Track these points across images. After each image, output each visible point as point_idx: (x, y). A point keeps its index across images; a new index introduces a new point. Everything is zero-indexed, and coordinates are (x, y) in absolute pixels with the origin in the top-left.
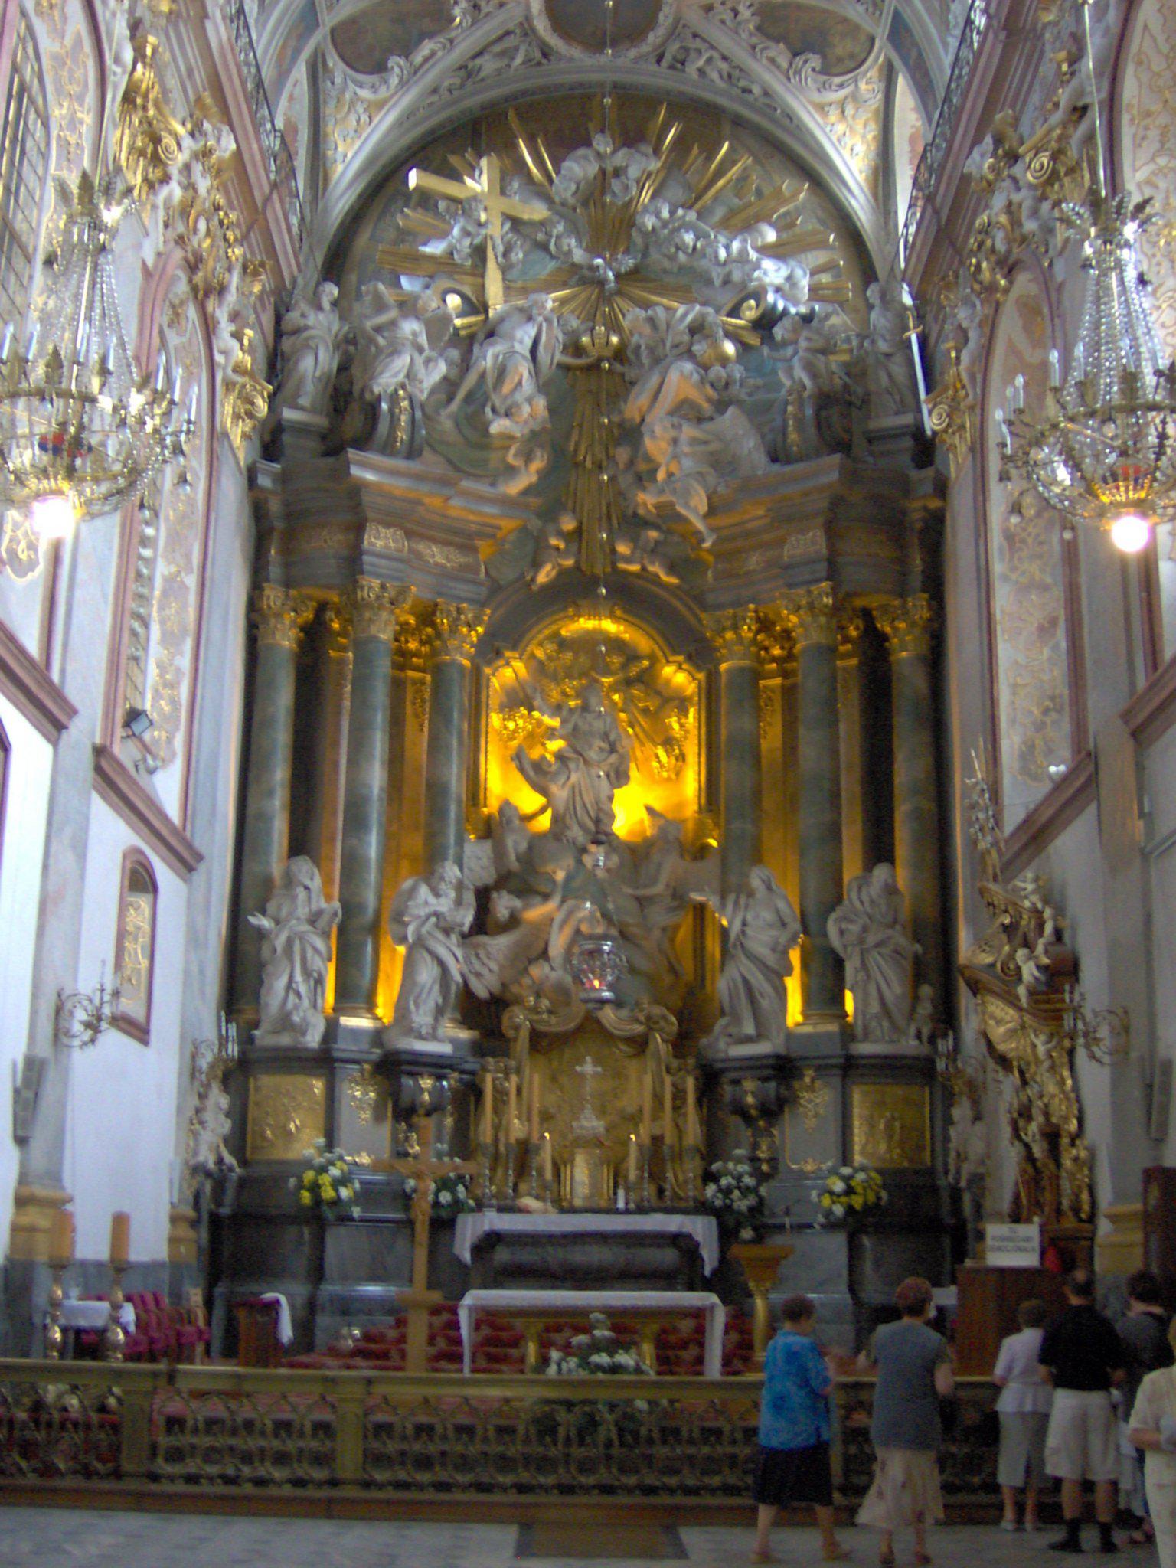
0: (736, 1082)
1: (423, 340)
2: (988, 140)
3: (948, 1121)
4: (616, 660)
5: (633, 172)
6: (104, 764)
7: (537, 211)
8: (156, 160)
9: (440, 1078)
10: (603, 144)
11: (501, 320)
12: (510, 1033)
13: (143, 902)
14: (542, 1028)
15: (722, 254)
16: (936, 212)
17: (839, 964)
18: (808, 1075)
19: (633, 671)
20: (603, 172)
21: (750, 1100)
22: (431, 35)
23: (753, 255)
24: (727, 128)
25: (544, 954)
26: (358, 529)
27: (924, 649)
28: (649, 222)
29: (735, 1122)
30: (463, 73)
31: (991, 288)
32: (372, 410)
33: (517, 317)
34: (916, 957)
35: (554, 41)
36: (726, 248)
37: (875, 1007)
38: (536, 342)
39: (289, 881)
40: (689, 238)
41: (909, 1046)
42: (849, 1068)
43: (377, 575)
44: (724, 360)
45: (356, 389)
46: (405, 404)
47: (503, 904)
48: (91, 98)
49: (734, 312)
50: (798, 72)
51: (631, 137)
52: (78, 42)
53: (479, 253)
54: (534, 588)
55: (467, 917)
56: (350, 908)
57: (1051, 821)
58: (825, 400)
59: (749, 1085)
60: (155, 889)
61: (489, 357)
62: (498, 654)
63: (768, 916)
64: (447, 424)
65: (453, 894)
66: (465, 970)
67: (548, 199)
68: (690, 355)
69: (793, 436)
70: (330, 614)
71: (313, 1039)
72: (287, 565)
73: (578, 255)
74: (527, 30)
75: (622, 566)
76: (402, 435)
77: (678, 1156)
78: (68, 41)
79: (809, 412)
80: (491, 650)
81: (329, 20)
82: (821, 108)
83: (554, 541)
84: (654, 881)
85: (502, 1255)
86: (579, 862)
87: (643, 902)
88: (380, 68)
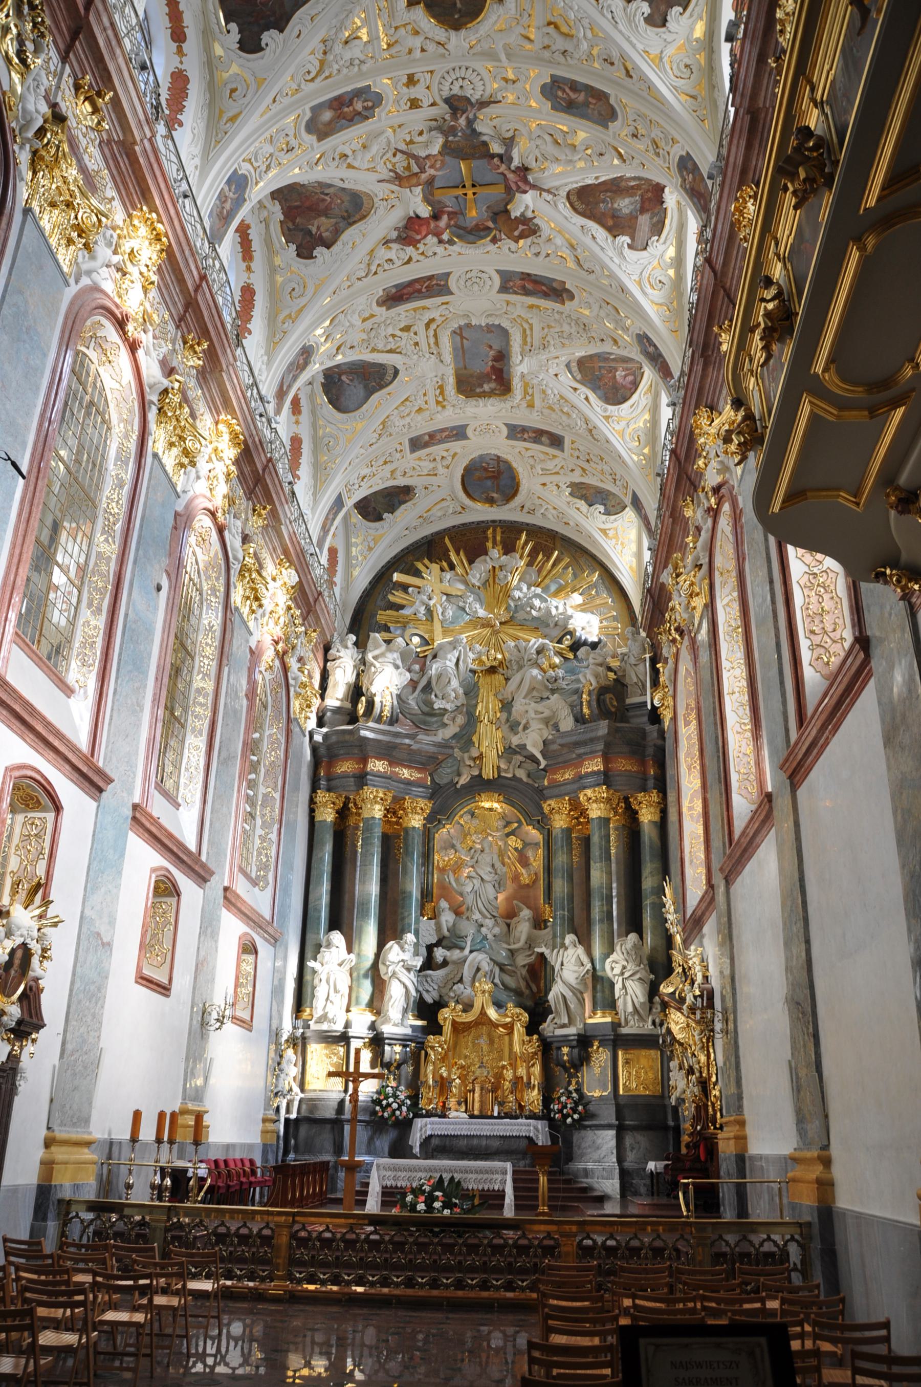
0: (559, 1048)
1: (399, 662)
2: (670, 566)
3: (669, 1070)
4: (501, 823)
5: (508, 568)
6: (228, 894)
8: (257, 599)
9: (405, 1046)
10: (495, 553)
11: (441, 646)
12: (442, 1023)
13: (251, 958)
14: (458, 1020)
16: (652, 597)
17: (612, 985)
18: (596, 1043)
19: (508, 830)
20: (494, 568)
21: (565, 1058)
22: (405, 502)
24: (558, 544)
25: (461, 981)
26: (364, 761)
27: (657, 818)
28: (517, 594)
29: (558, 1070)
30: (421, 520)
31: (674, 641)
33: (449, 647)
34: (652, 981)
35: (467, 501)
36: (557, 606)
37: (630, 1009)
38: (458, 660)
39: (329, 945)
40: (537, 603)
41: (648, 1027)
43: (374, 786)
44: (553, 667)
45: (364, 690)
47: (440, 954)
48: (222, 580)
49: (560, 641)
50: (592, 514)
51: (509, 548)
52: (216, 554)
54: (458, 786)
55: (418, 962)
57: (703, 914)
58: (602, 691)
59: (565, 1050)
60: (256, 953)
61: (434, 668)
62: (440, 821)
64: (413, 703)
65: (412, 950)
66: (420, 989)
67: (466, 583)
69: (586, 710)
70: (351, 805)
72: (329, 780)
73: (481, 613)
75: (503, 774)
77: (529, 1086)
78: (212, 555)
79: (594, 697)
81: (349, 503)
82: (604, 531)
83: (468, 763)
84: (519, 940)
85: (435, 1142)
86: (479, 931)
87: (512, 952)
88: (379, 518)
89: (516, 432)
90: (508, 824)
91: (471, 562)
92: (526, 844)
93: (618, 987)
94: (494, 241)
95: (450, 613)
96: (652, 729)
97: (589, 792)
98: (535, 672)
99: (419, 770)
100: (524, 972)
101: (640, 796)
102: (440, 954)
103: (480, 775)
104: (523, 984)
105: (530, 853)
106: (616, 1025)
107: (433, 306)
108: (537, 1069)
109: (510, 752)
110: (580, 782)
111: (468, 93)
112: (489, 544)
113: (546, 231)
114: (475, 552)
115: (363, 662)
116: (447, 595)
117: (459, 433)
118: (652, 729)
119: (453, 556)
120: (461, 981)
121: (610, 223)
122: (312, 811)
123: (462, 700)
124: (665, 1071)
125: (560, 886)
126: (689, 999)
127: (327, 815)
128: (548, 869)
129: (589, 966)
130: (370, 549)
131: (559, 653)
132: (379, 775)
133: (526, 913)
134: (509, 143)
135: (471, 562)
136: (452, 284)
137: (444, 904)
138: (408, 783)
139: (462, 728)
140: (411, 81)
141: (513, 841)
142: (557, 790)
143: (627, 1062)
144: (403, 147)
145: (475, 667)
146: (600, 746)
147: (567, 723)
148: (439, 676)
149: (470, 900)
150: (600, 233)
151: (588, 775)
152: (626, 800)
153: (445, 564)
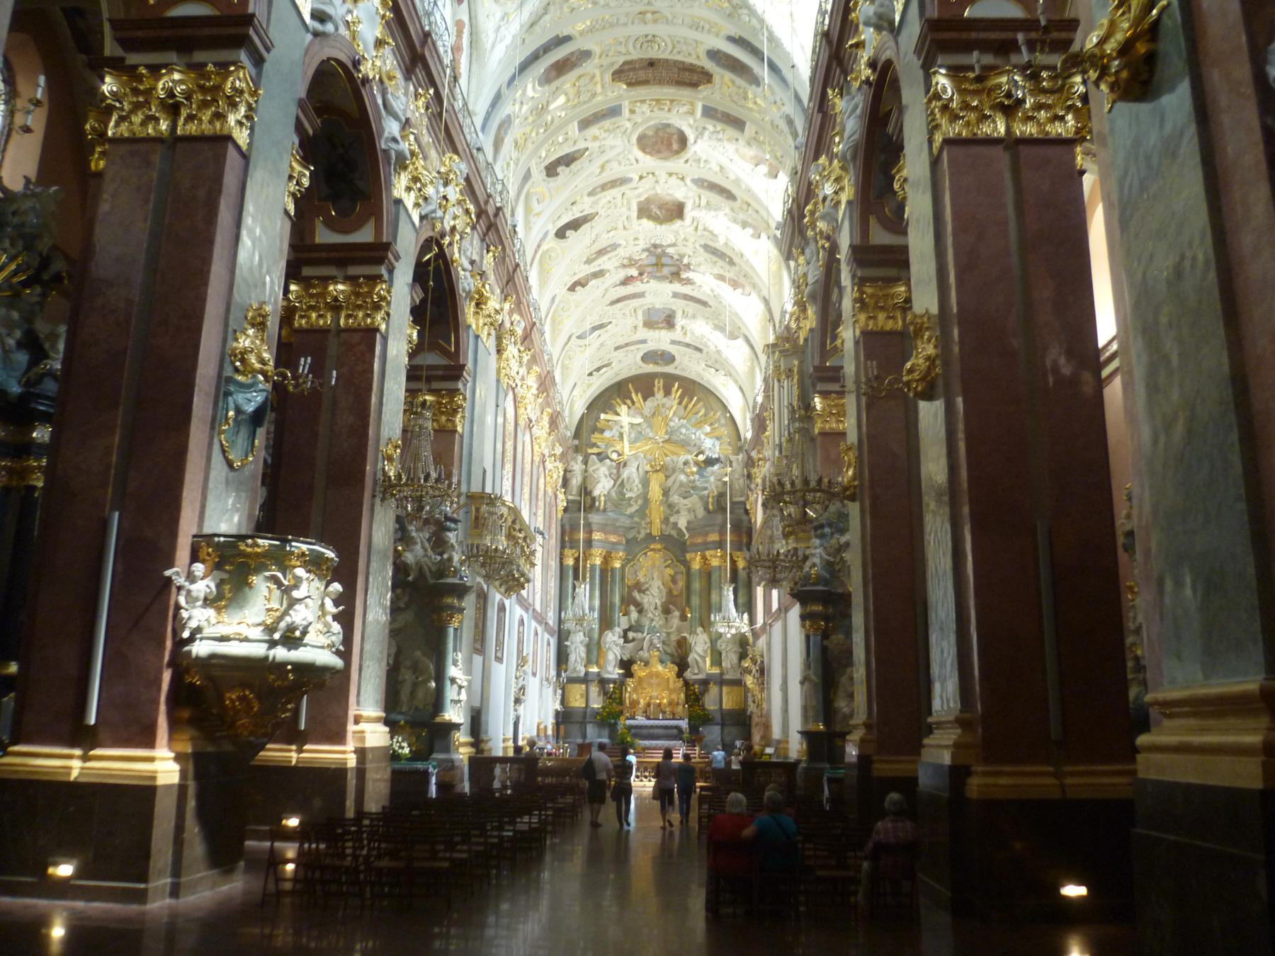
5: (667, 406)
7: (639, 420)
10: (659, 395)
15: (693, 437)
17: (720, 654)
23: (703, 437)
25: (642, 649)
28: (672, 424)
32: (594, 499)
40: (684, 431)
41: (737, 676)
42: (721, 682)
44: (692, 473)
46: (603, 498)
47: (631, 635)
49: (697, 456)
53: (621, 435)
55: (622, 641)
56: (591, 639)
59: (697, 686)
61: (625, 474)
63: (702, 641)
64: (613, 494)
67: (642, 415)
68: (683, 471)
69: (711, 507)
71: (582, 674)
74: (636, 363)
76: (602, 507)
77: (678, 704)
87: (668, 634)
89: (673, 342)
90: (666, 561)
91: (645, 399)
93: (723, 655)
94: (671, 282)
95: (633, 435)
97: (712, 552)
98: (682, 477)
99: (619, 535)
100: (675, 644)
102: (631, 635)
104: (674, 650)
106: (722, 674)
107: (634, 303)
108: (682, 696)
109: (666, 520)
110: (706, 546)
111: (665, 244)
112: (656, 389)
113: (698, 284)
114: (648, 394)
115: (586, 471)
116: (632, 424)
117: (644, 342)
119: (633, 395)
120: (642, 649)
122: (561, 559)
123: (641, 490)
124: (746, 698)
125: (695, 601)
126: (754, 671)
127: (570, 562)
129: (709, 644)
130: (584, 391)
131: (696, 463)
132: (598, 541)
133: (677, 613)
134: (682, 256)
135: (645, 399)
136: (646, 294)
137: (632, 608)
138: (613, 543)
139: (641, 506)
140: (636, 239)
143: (728, 693)
144: (627, 256)
145: (648, 468)
146: (717, 528)
147: (701, 513)
148: (629, 478)
149: (646, 606)
151: (710, 543)
153: (629, 402)
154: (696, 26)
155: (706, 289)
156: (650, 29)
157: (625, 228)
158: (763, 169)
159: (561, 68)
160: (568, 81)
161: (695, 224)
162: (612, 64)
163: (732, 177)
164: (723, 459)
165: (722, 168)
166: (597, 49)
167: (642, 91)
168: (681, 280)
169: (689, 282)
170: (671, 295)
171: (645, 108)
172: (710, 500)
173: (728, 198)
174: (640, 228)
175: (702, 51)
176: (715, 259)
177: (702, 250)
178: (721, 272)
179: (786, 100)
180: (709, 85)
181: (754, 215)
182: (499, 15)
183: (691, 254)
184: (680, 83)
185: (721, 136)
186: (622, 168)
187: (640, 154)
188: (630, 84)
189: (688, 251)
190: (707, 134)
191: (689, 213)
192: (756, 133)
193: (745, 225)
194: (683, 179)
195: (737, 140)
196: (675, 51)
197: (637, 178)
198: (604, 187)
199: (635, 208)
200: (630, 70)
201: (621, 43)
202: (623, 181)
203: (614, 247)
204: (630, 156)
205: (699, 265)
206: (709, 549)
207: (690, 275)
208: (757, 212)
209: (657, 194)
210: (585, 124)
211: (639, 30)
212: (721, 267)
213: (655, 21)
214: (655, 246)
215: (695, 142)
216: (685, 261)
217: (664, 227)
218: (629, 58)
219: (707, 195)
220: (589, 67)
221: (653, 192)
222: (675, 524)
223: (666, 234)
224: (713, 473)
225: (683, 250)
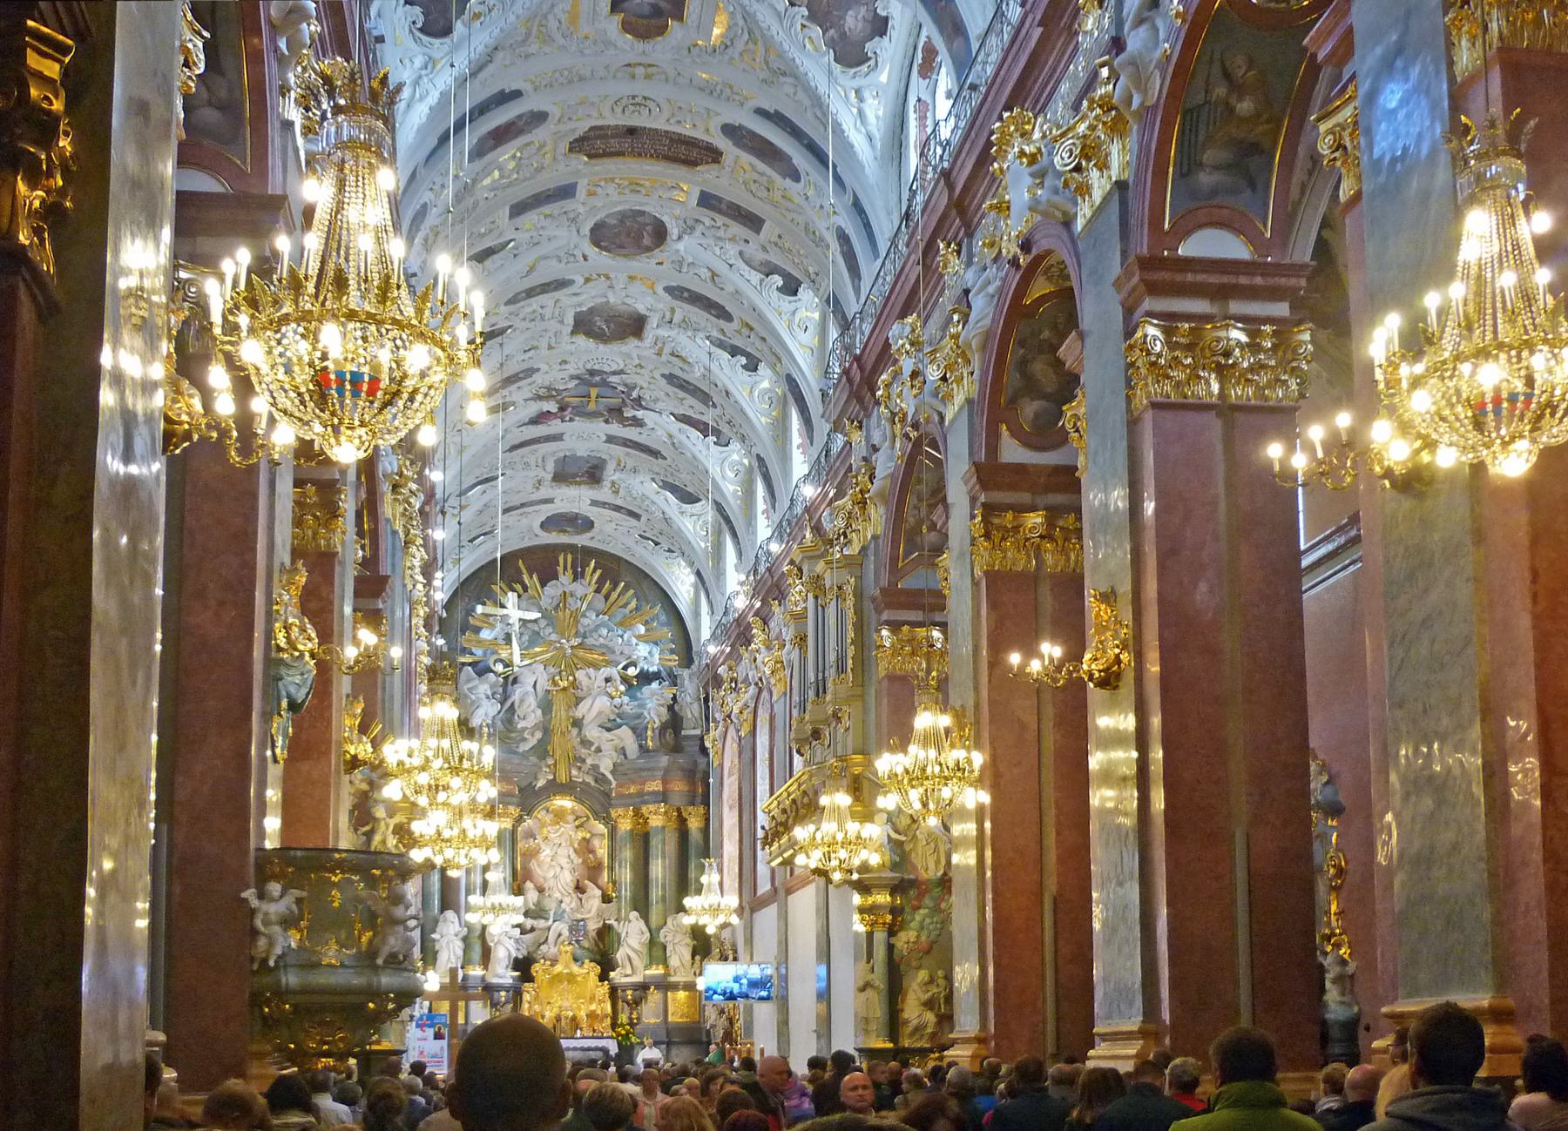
4: (573, 817)
58: (664, 728)
69: (650, 743)
80: (519, 820)
92: (593, 835)
94: (607, 422)
96: (701, 760)
98: (605, 699)
101: (690, 809)
103: (555, 779)
105: (596, 842)
113: (650, 424)
118: (701, 760)
121: (702, 427)
128: (612, 857)
141: (580, 835)
142: (625, 800)
146: (660, 773)
150: (695, 434)
151: (650, 793)
152: (679, 810)
154: (709, 90)
155: (660, 432)
156: (641, 88)
157: (550, 348)
158: (778, 280)
159: (500, 136)
160: (506, 155)
161: (660, 345)
162: (574, 130)
163: (730, 288)
164: (664, 674)
165: (714, 275)
166: (554, 111)
167: (610, 166)
168: (623, 421)
169: (638, 423)
170: (604, 438)
171: (611, 189)
172: (649, 733)
173: (718, 317)
174: (573, 346)
175: (715, 124)
176: (681, 394)
177: (664, 382)
178: (690, 413)
179: (839, 209)
180: (715, 166)
181: (758, 343)
182: (419, 61)
183: (645, 385)
184: (667, 158)
185: (721, 233)
186: (562, 265)
187: (592, 251)
188: (590, 156)
189: (640, 381)
190: (700, 228)
191: (651, 332)
192: (780, 237)
193: (734, 351)
194: (652, 287)
195: (747, 241)
196: (672, 121)
197: (580, 280)
198: (530, 293)
199: (570, 320)
200: (597, 138)
201: (593, 104)
202: (561, 284)
203: (531, 372)
204: (578, 253)
205: (656, 400)
206: (646, 803)
207: (640, 414)
208: (764, 339)
209: (608, 302)
210: (518, 209)
211: (624, 88)
212: (691, 406)
213: (648, 77)
214: (592, 373)
215: (680, 238)
216: (635, 394)
217: (616, 347)
218: (600, 123)
219: (684, 310)
220: (540, 134)
221: (604, 300)
222: (595, 767)
223: (610, 356)
224: (653, 694)
225: (629, 380)
